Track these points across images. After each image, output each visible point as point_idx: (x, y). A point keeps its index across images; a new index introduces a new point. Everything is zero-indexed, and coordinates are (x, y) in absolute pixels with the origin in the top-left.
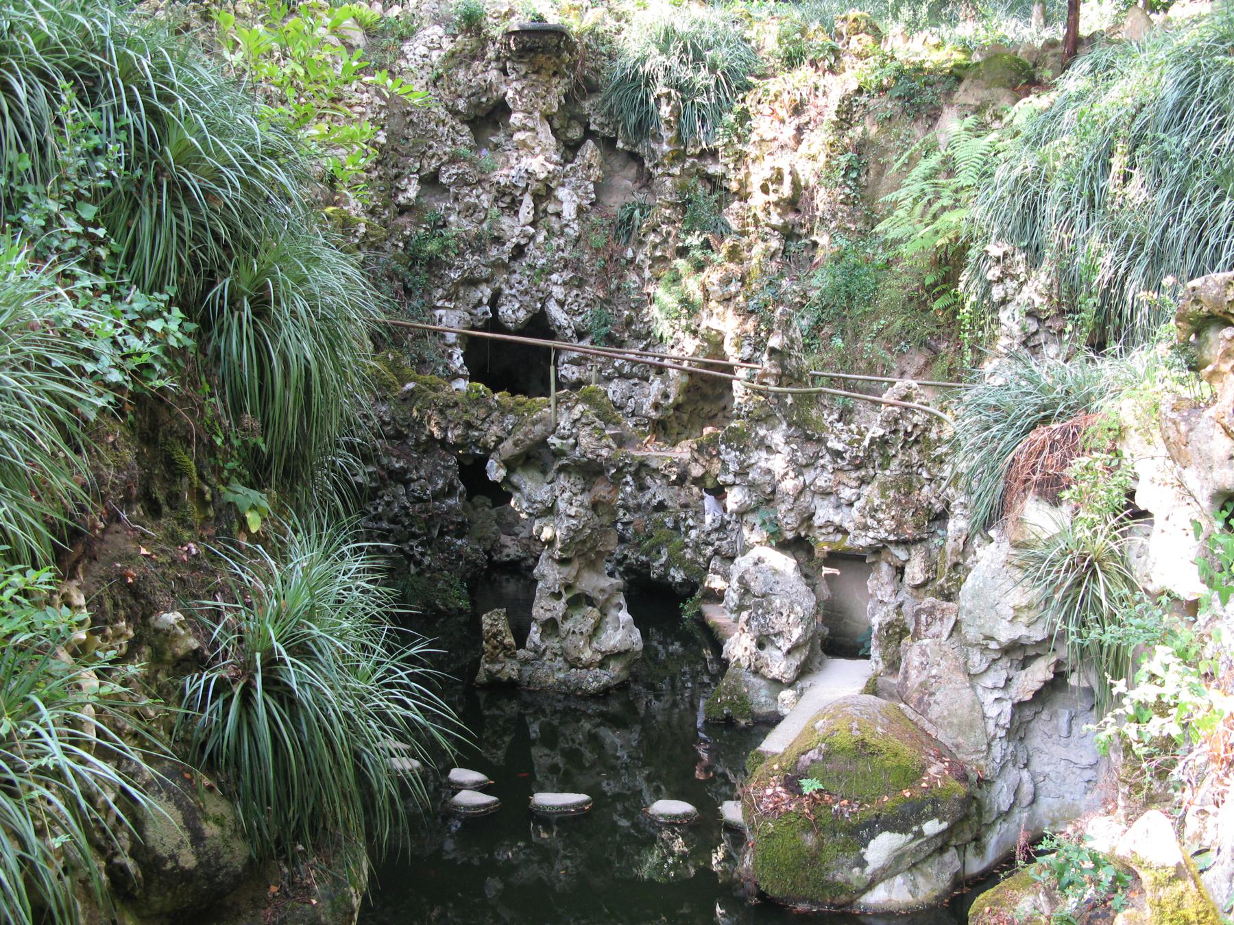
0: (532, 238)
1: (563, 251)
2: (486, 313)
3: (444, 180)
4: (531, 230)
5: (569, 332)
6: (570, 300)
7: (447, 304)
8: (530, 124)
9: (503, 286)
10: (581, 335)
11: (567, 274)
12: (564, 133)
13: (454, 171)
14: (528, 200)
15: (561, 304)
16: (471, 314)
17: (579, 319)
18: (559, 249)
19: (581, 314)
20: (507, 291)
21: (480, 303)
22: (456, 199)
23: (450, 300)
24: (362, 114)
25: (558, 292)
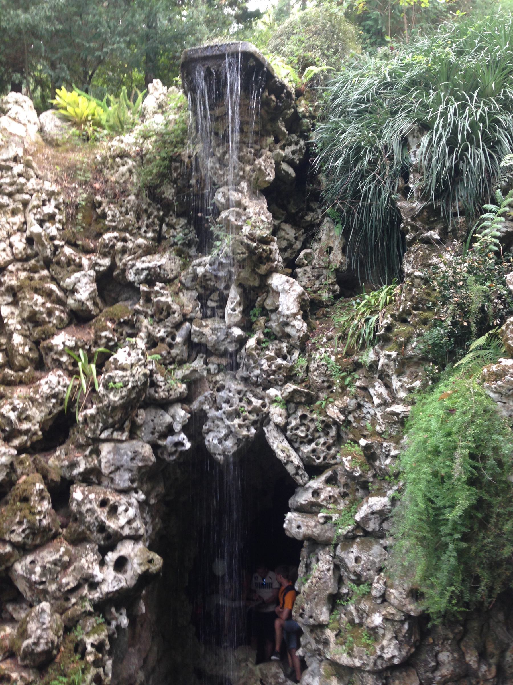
0: (242, 341)
1: (285, 358)
2: (180, 444)
3: (131, 276)
4: (237, 332)
5: (290, 469)
6: (294, 423)
7: (116, 435)
8: (235, 196)
9: (206, 407)
10: (313, 470)
11: (290, 387)
12: (303, 217)
13: (144, 265)
14: (234, 295)
15: (282, 429)
16: (155, 447)
17: (306, 449)
18: (279, 354)
19: (310, 442)
20: (212, 413)
21: (170, 430)
22: (148, 300)
23: (121, 429)
24: (25, 204)
25: (277, 414)
